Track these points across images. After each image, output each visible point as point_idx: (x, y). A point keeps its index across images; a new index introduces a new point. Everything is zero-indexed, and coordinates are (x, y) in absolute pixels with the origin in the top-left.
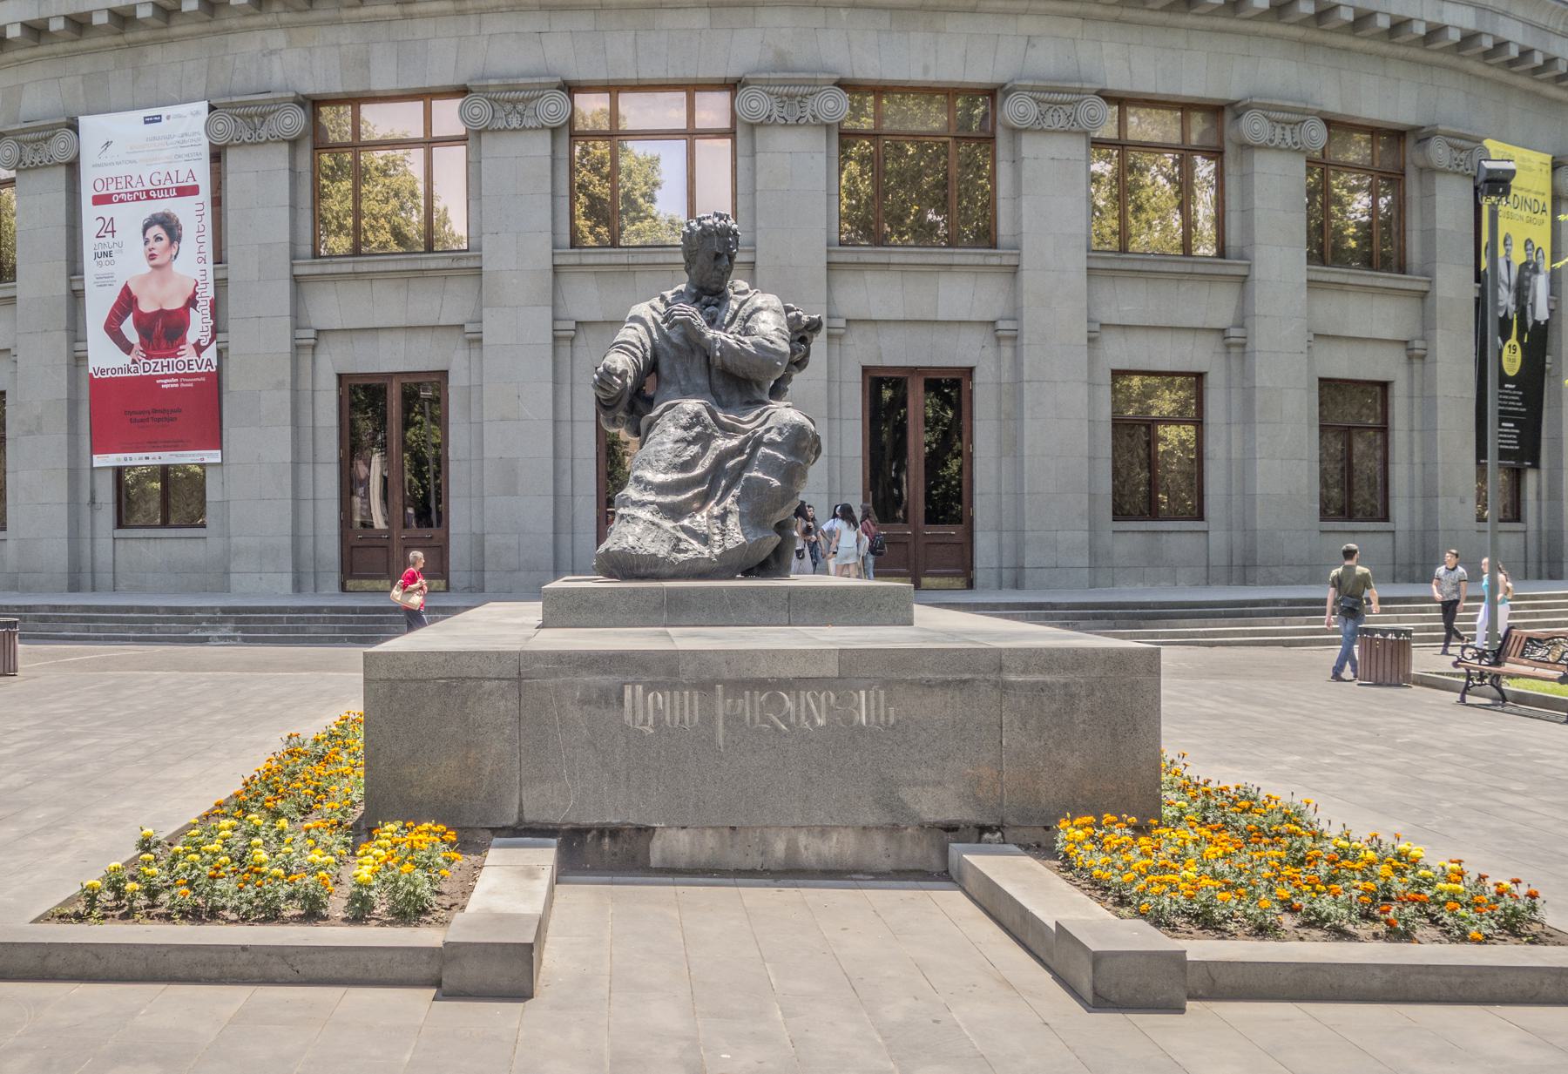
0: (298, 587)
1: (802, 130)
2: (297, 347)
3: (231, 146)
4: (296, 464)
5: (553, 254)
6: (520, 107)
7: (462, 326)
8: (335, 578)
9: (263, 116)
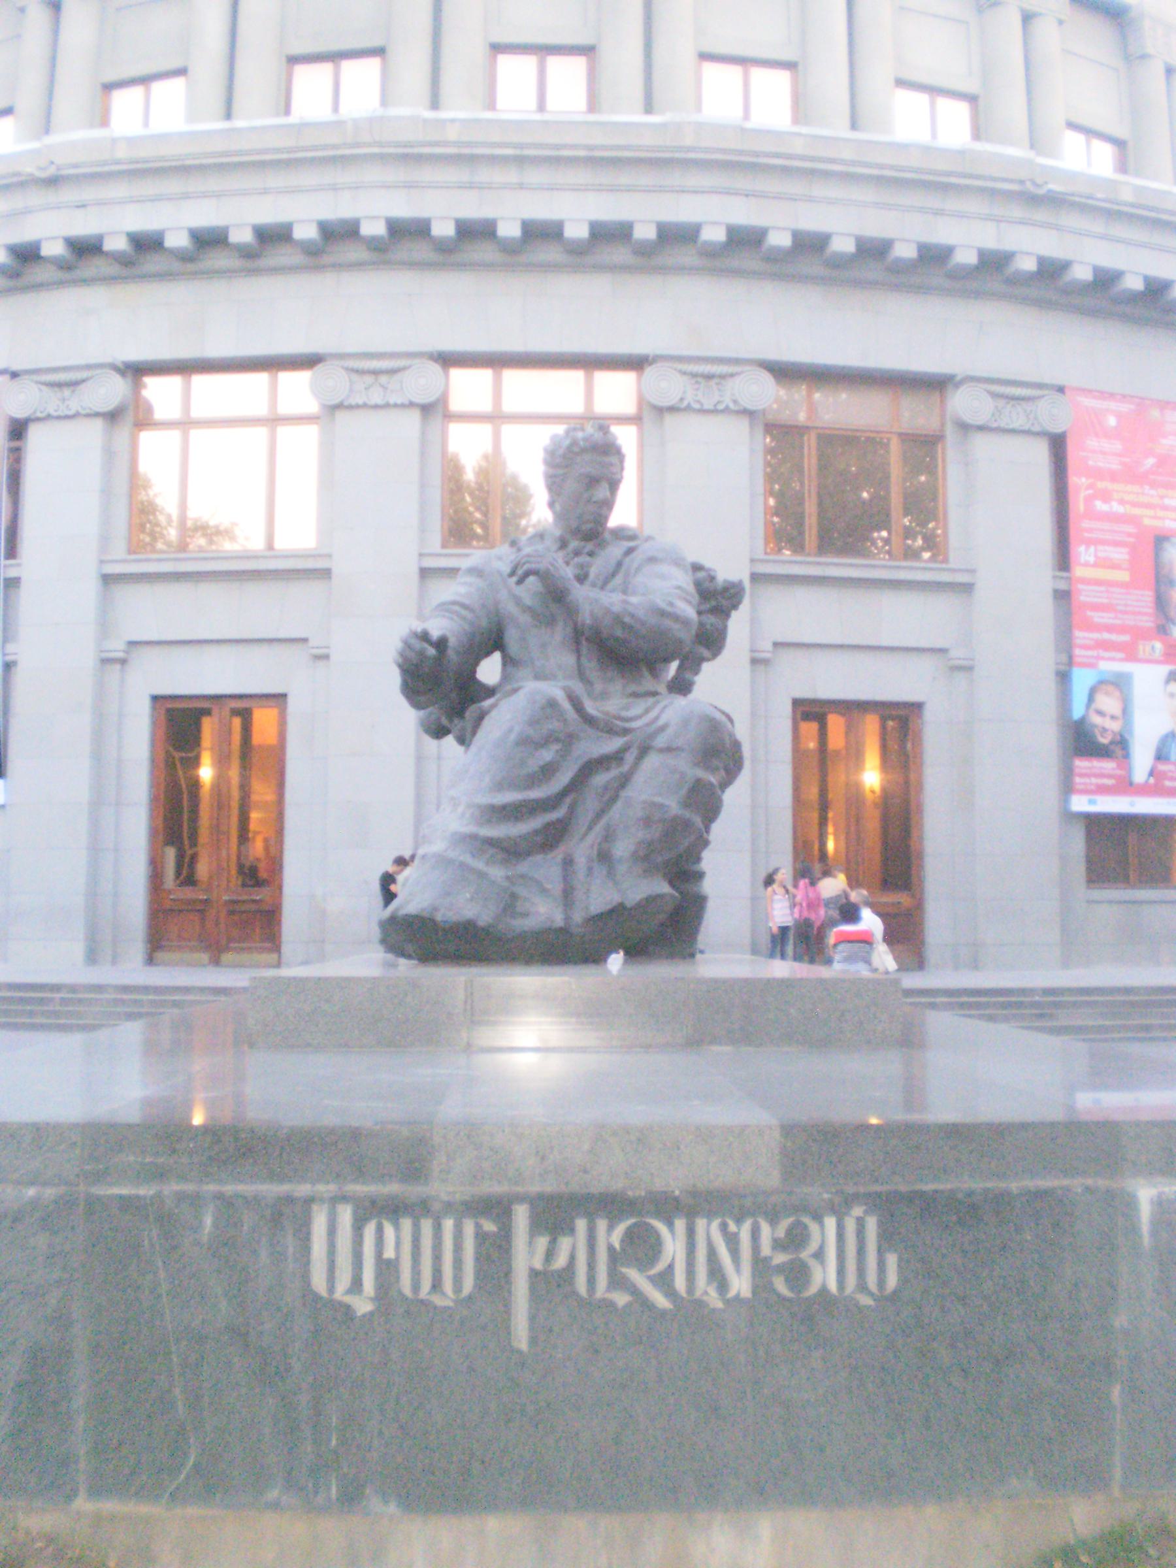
0: (92, 957)
1: (719, 419)
2: (105, 661)
3: (38, 419)
4: (97, 803)
5: (421, 555)
6: (383, 379)
7: (305, 640)
8: (137, 948)
9: (74, 384)
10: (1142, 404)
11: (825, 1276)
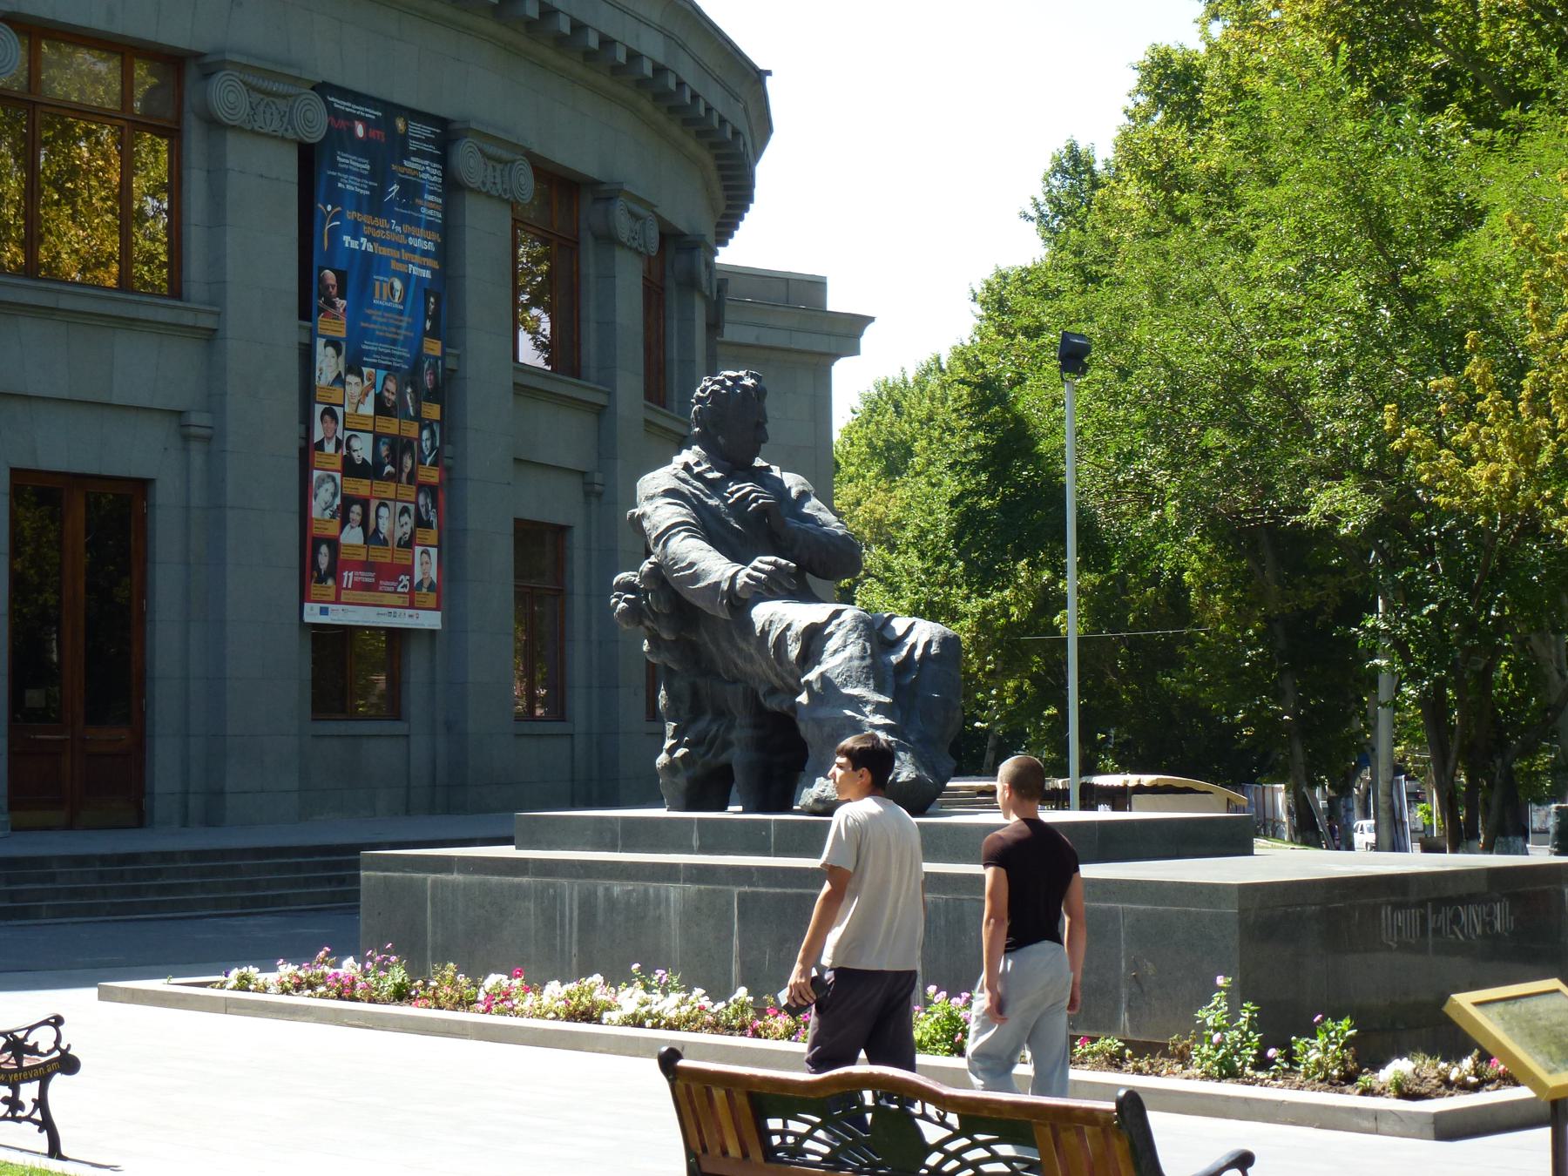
10: (391, 109)
11: (1498, 926)
